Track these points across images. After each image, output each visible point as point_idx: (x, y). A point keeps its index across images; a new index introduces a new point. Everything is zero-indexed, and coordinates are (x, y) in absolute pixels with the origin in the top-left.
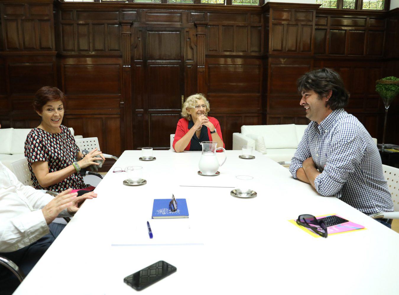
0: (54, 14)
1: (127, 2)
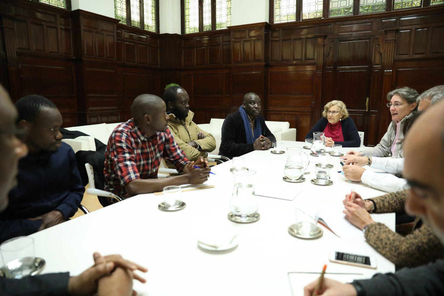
0: (265, 34)
1: (323, 18)
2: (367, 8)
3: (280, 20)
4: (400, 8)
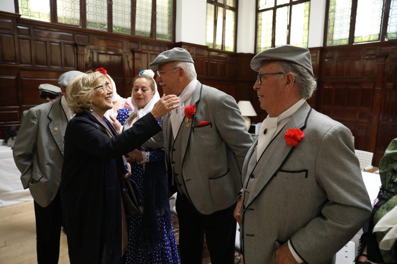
1: (80, 27)
2: (118, 29)
3: (29, 15)
4: (139, 35)
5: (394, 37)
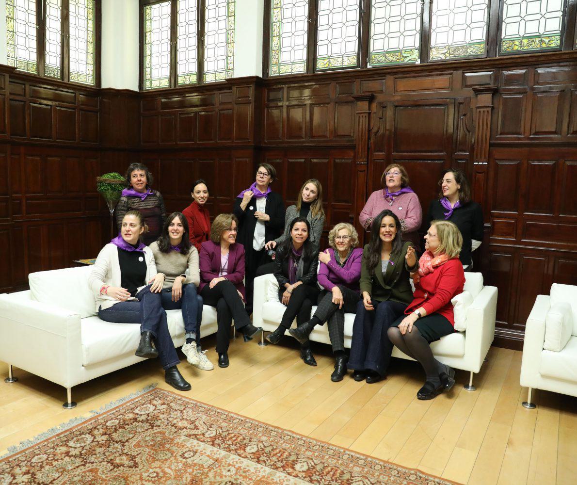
5: (382, 63)
